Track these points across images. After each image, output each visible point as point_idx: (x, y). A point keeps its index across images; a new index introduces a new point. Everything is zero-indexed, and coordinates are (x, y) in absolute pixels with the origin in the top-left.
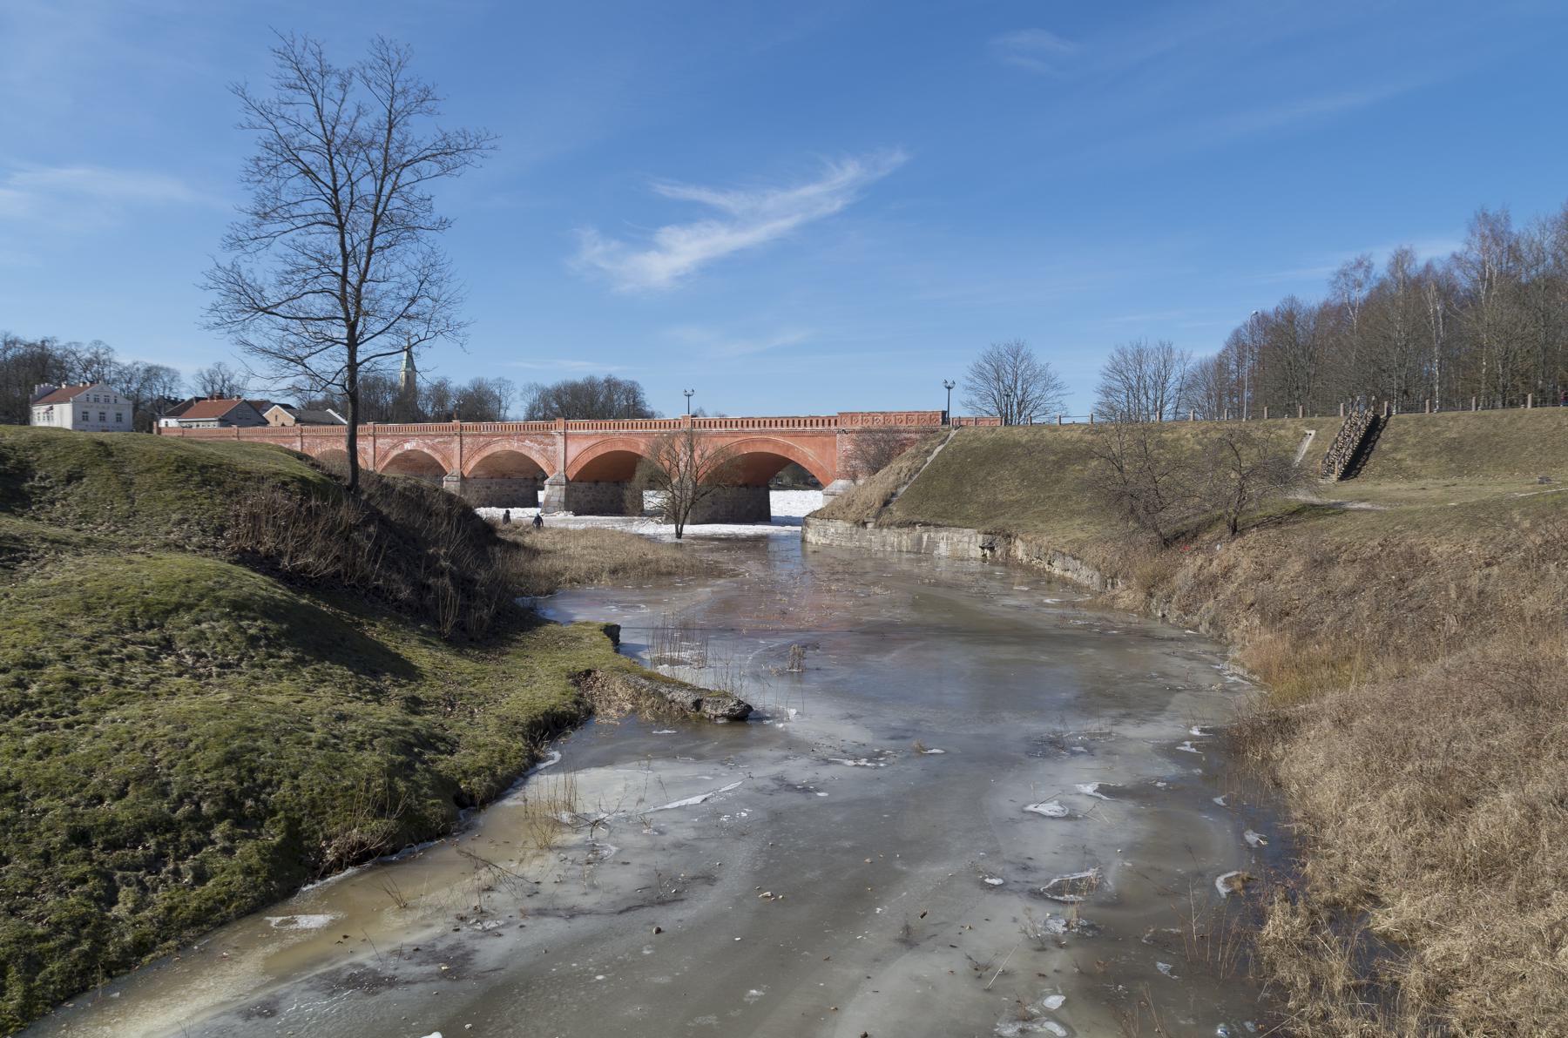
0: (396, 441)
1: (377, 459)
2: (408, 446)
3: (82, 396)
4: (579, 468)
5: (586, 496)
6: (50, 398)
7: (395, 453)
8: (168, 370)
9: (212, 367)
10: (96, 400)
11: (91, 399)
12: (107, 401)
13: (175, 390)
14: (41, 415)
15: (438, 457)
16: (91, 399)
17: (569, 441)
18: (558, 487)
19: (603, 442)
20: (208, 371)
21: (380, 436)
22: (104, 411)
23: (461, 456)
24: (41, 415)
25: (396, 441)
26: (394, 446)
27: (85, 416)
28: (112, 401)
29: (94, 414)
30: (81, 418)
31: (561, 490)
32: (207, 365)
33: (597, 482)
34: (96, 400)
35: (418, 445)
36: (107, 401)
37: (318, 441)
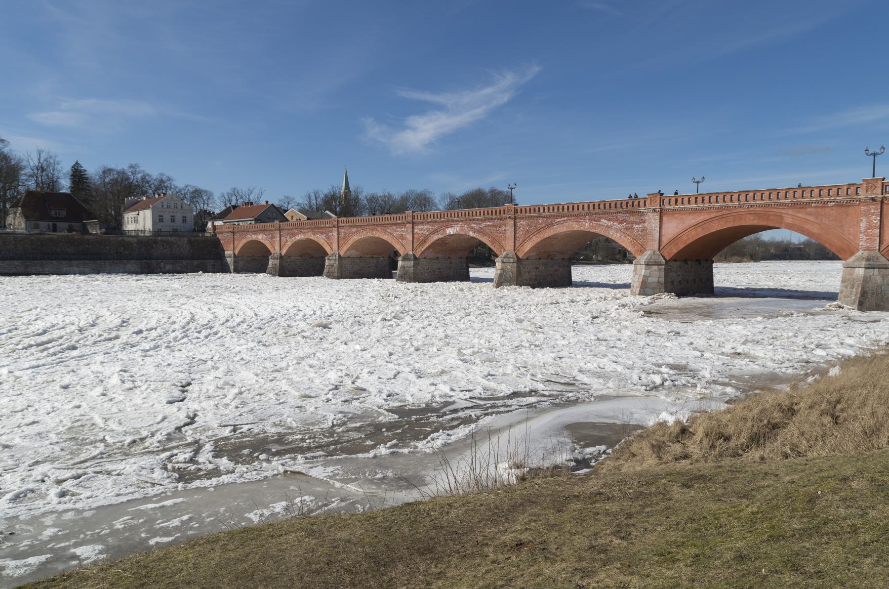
0: (436, 227)
1: (416, 244)
2: (450, 231)
3: (158, 204)
4: (682, 246)
5: (678, 275)
6: (135, 206)
7: (435, 237)
8: (206, 191)
9: (229, 191)
10: (168, 207)
11: (165, 206)
12: (176, 207)
13: (210, 205)
14: (130, 220)
15: (485, 240)
16: (165, 206)
17: (665, 219)
18: (655, 268)
19: (722, 217)
20: (228, 194)
21: (418, 223)
22: (173, 215)
23: (515, 238)
24: (130, 220)
25: (436, 227)
26: (435, 232)
27: (161, 219)
28: (179, 207)
29: (167, 217)
30: (158, 219)
31: (660, 270)
32: (227, 190)
33: (686, 261)
34: (168, 207)
35: (462, 229)
36: (176, 207)
37: (354, 230)
